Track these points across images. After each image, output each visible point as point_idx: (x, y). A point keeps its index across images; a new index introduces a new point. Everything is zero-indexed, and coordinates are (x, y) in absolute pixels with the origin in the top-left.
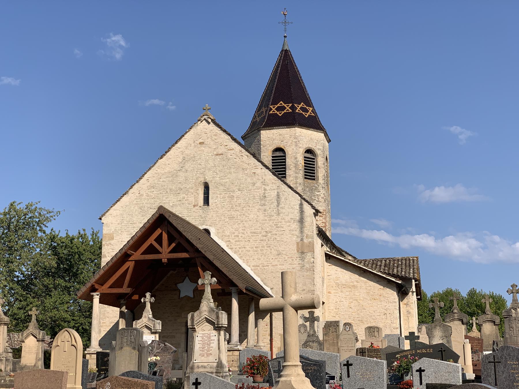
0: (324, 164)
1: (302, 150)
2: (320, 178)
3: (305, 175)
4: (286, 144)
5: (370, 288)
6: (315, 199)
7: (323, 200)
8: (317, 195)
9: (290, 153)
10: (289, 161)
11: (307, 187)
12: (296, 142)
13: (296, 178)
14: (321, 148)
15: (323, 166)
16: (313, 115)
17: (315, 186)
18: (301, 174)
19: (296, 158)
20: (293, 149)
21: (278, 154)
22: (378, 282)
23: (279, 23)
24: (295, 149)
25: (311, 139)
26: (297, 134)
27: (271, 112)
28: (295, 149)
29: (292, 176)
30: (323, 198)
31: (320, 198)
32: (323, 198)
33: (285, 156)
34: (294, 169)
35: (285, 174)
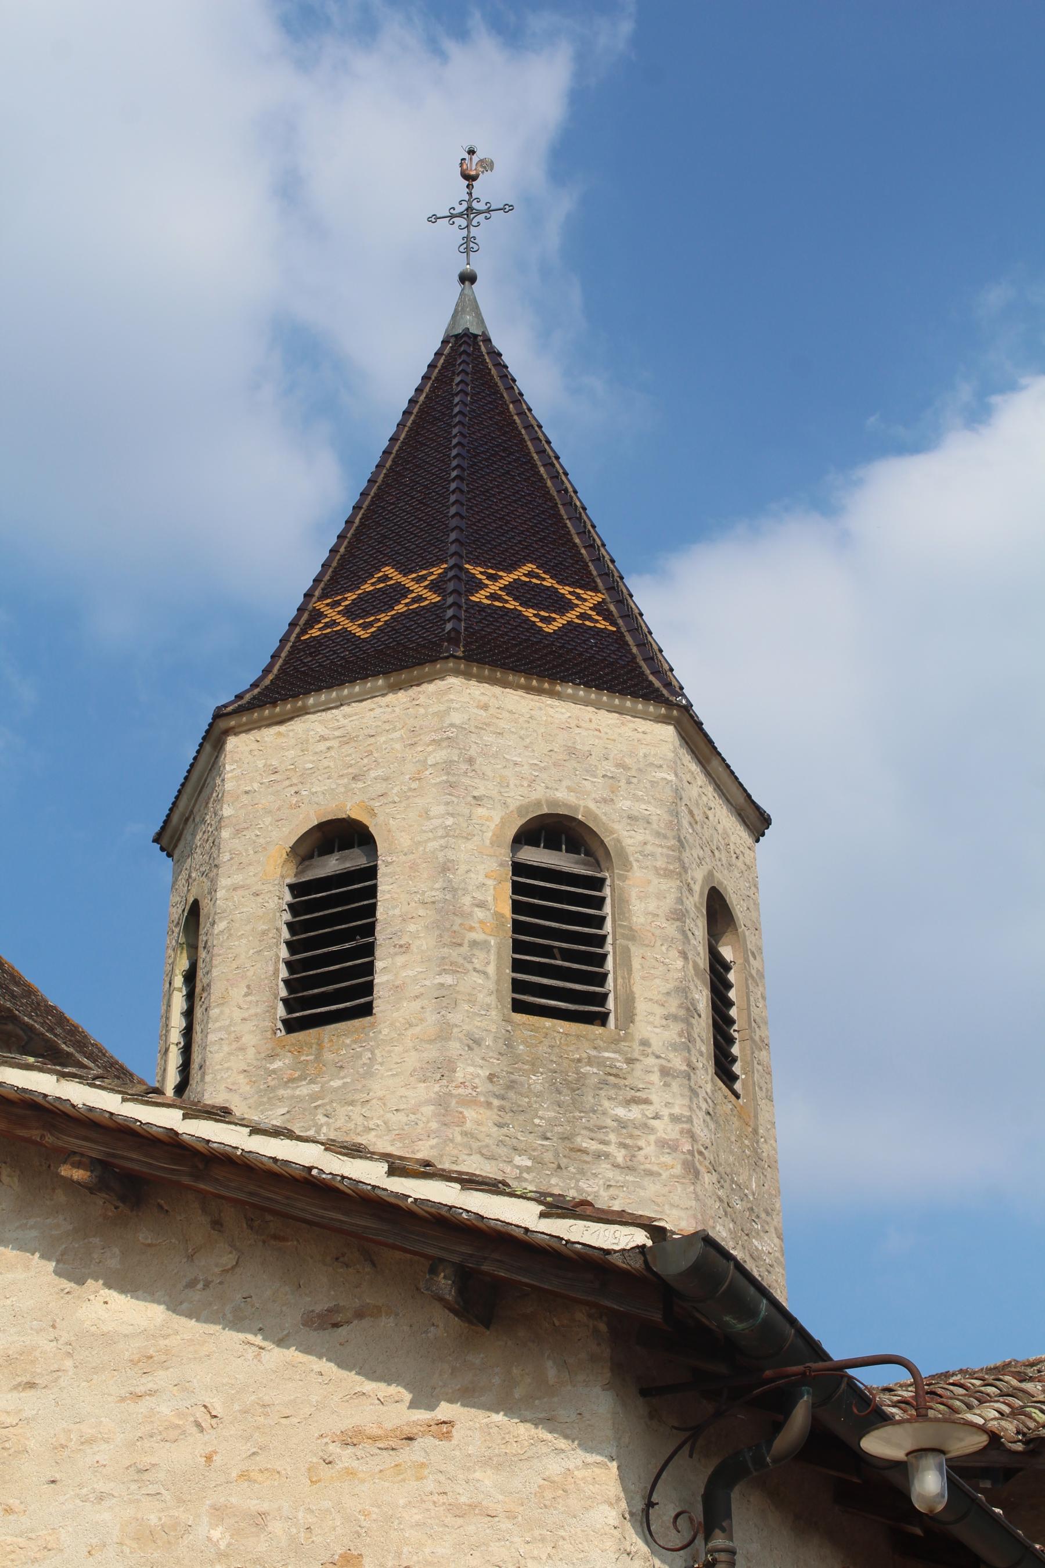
0: (679, 915)
1: (496, 821)
2: (641, 1007)
3: (518, 986)
4: (381, 787)
5: (184, 1455)
6: (598, 1156)
7: (672, 1164)
8: (623, 1124)
9: (404, 840)
10: (400, 901)
11: (535, 1065)
12: (447, 766)
13: (445, 999)
14: (657, 813)
15: (671, 929)
16: (602, 624)
17: (601, 1063)
18: (490, 968)
19: (445, 868)
20: (426, 814)
21: (332, 865)
22: (322, 1328)
23: (434, 219)
24: (437, 810)
25: (571, 752)
26: (456, 718)
27: (315, 632)
28: (437, 810)
29: (417, 989)
30: (666, 1145)
31: (649, 1148)
32: (666, 1145)
33: (371, 872)
34: (424, 943)
35: (368, 989)
